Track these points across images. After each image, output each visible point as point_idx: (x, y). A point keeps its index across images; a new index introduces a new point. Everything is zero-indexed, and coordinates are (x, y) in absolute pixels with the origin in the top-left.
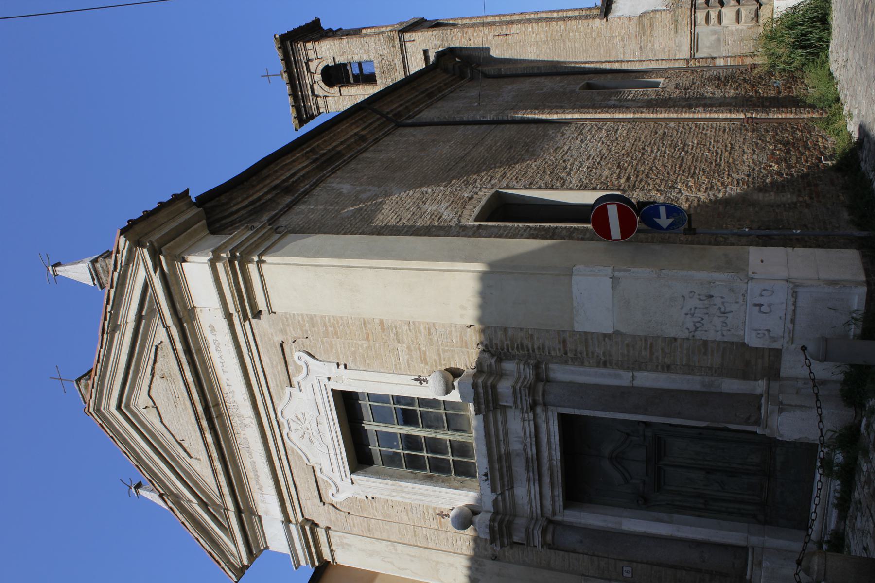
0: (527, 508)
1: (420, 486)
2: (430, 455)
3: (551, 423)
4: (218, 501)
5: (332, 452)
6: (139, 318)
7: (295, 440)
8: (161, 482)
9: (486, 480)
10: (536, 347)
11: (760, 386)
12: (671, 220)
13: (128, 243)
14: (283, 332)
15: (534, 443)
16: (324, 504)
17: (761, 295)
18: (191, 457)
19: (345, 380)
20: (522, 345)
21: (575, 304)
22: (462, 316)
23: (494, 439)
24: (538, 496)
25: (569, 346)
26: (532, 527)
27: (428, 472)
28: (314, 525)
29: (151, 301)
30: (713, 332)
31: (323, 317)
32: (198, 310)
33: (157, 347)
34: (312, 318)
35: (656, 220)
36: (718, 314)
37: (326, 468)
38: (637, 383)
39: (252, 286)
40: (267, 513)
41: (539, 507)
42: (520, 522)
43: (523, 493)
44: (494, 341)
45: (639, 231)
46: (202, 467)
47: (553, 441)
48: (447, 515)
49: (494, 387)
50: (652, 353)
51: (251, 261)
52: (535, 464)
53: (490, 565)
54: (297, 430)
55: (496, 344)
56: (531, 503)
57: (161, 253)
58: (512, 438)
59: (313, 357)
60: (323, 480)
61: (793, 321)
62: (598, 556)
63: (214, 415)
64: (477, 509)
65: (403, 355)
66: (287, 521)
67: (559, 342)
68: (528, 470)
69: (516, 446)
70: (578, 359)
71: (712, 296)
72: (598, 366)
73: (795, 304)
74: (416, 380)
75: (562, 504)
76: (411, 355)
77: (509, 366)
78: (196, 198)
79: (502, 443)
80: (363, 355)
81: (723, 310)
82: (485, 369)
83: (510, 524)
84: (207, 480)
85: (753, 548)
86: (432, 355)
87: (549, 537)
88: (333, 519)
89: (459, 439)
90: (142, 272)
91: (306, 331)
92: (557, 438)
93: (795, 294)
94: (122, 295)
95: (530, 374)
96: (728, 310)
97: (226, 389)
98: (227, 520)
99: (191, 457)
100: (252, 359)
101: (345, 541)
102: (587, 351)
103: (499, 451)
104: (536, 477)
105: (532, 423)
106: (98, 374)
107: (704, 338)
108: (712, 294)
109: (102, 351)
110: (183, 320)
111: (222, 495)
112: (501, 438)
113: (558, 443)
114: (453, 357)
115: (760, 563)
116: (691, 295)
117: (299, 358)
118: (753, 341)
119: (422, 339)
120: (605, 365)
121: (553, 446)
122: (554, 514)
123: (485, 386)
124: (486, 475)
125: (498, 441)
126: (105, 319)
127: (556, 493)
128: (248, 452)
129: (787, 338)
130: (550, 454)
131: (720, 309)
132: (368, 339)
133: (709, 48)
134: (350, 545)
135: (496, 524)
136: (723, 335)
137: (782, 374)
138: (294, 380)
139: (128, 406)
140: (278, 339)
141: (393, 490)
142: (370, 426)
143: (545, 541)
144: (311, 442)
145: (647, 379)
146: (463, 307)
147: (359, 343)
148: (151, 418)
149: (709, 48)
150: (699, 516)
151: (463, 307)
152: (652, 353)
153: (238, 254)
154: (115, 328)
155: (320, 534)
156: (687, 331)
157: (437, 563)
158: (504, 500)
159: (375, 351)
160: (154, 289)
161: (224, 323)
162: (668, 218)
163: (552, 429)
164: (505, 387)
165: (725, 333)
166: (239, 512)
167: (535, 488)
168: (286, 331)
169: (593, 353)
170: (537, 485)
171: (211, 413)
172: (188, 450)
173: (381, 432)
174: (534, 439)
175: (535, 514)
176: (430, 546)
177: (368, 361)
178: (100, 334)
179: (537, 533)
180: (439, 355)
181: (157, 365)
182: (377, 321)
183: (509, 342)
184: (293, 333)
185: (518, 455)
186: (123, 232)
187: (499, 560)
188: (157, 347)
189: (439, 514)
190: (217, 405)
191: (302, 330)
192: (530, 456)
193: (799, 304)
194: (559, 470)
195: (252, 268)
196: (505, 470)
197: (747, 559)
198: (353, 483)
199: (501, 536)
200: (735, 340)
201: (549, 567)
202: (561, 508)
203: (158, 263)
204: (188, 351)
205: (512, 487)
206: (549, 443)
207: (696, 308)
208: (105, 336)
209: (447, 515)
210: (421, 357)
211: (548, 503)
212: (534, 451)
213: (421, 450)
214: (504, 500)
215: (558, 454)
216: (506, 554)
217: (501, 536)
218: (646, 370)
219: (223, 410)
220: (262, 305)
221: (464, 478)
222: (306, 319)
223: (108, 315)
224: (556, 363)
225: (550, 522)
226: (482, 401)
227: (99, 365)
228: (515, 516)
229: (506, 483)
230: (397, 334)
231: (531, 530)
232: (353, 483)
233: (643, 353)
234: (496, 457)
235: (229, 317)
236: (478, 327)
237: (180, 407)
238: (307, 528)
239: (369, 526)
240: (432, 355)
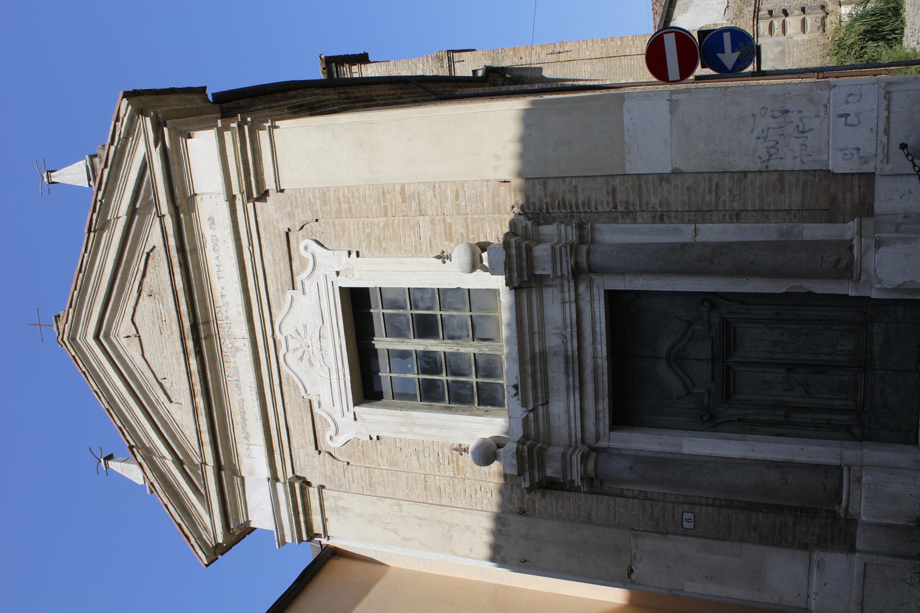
0: (564, 431)
1: (435, 414)
2: (450, 378)
3: (596, 303)
4: (197, 461)
5: (334, 376)
6: (133, 211)
7: (293, 365)
8: (132, 431)
9: (516, 394)
10: (580, 202)
11: (849, 229)
12: (737, 54)
13: (130, 107)
14: (291, 215)
15: (575, 334)
16: (320, 452)
17: (847, 102)
18: (171, 402)
19: (356, 274)
20: (564, 202)
21: (626, 138)
22: (495, 168)
23: (526, 330)
24: (578, 411)
25: (620, 197)
26: (569, 453)
27: (446, 404)
28: (306, 483)
29: (147, 190)
30: (790, 159)
31: (337, 190)
32: (198, 198)
33: (148, 255)
34: (324, 193)
35: (719, 55)
36: (796, 134)
37: (326, 400)
38: (700, 238)
39: (260, 159)
40: (251, 473)
41: (579, 429)
42: (555, 451)
43: (561, 409)
44: (532, 200)
45: (699, 78)
46: (183, 415)
47: (598, 330)
48: (466, 450)
49: (529, 250)
50: (717, 198)
51: (264, 129)
52: (575, 362)
53: (517, 523)
54: (295, 350)
55: (534, 204)
56: (569, 422)
57: (166, 126)
58: (549, 330)
59: (322, 246)
60: (321, 417)
61: (887, 132)
62: (652, 500)
63: (202, 335)
64: (501, 442)
65: (425, 231)
66: (274, 479)
67: (608, 193)
68: (567, 373)
69: (553, 342)
70: (629, 214)
71: (787, 111)
72: (654, 222)
73: (888, 108)
74: (439, 257)
75: (607, 422)
76: (434, 230)
77: (548, 230)
78: (214, 95)
79: (536, 337)
80: (379, 237)
81: (801, 129)
82: (520, 231)
83: (542, 452)
84: (187, 432)
85: (849, 468)
86: (458, 228)
87: (591, 465)
88: (329, 473)
89: (486, 350)
90: (143, 148)
91: (317, 211)
92: (603, 326)
93: (888, 95)
94: (116, 179)
95: (572, 235)
96: (807, 127)
97: (219, 301)
98: (204, 478)
99: (171, 402)
100: (251, 244)
101: (341, 503)
102: (640, 201)
104: (577, 384)
105: (573, 305)
106: (78, 288)
107: (780, 168)
108: (787, 108)
109: (86, 255)
110: (181, 209)
111: (201, 444)
112: (536, 329)
113: (604, 332)
114: (483, 228)
115: (859, 480)
116: (763, 112)
117: (306, 248)
118: (839, 165)
119: (449, 207)
120: (662, 220)
121: (598, 338)
122: (598, 438)
123: (518, 247)
124: (516, 387)
125: (532, 334)
126: (94, 211)
127: (601, 407)
128: (237, 386)
129: (881, 156)
130: (595, 349)
131: (798, 127)
132: (386, 215)
133: (773, 60)
134: (345, 509)
135: (526, 448)
136: (803, 162)
137: (875, 211)
138: (298, 279)
139: (107, 336)
140: (283, 227)
141: (403, 424)
142: (382, 343)
143: (585, 469)
144: (311, 364)
145: (713, 232)
146: (497, 157)
147: (376, 220)
148: (131, 351)
149: (773, 60)
150: (778, 435)
151: (497, 157)
152: (717, 198)
153: (249, 119)
154: (104, 225)
155: (311, 496)
156: (759, 161)
157: (451, 526)
158: (536, 419)
159: (393, 230)
160: (152, 172)
161: (225, 206)
162: (733, 51)
163: (597, 313)
164: (541, 252)
165: (805, 159)
166: (219, 468)
167: (575, 400)
168: (293, 214)
169: (647, 204)
170: (577, 396)
171: (199, 334)
172: (169, 393)
173: (394, 350)
174: (575, 329)
175: (574, 440)
176: (443, 503)
177: (384, 245)
178: (86, 231)
179: (576, 458)
180: (467, 226)
181: (146, 280)
182: (398, 188)
183: (549, 200)
184: (301, 215)
185: (555, 354)
186: (127, 95)
187: (527, 515)
188: (148, 255)
189: (456, 450)
190: (207, 323)
191: (311, 210)
192: (570, 353)
193: (894, 108)
194: (605, 371)
195: (263, 136)
196: (539, 376)
197: (841, 479)
198: (355, 419)
199: (533, 357)
200: (817, 167)
201: (589, 521)
202: (607, 429)
203: (160, 136)
204: (181, 249)
205: (547, 403)
206: (594, 332)
207: (768, 129)
208: (92, 234)
209: (466, 450)
210: (445, 232)
213: (439, 372)
214: (536, 419)
215: (605, 348)
216: (537, 506)
217: (532, 466)
218: (711, 222)
219: (214, 330)
220: (270, 184)
221: (489, 407)
222: (318, 195)
223: (98, 204)
224: (604, 222)
225: (593, 449)
226: (515, 266)
227: (81, 275)
228: (550, 445)
229: (540, 395)
230: (419, 204)
231: (568, 456)
232: (355, 419)
233: (707, 198)
234: (528, 356)
235: (231, 199)
236: (516, 182)
237: (166, 333)
238: (297, 485)
239: (371, 478)
240: (458, 228)
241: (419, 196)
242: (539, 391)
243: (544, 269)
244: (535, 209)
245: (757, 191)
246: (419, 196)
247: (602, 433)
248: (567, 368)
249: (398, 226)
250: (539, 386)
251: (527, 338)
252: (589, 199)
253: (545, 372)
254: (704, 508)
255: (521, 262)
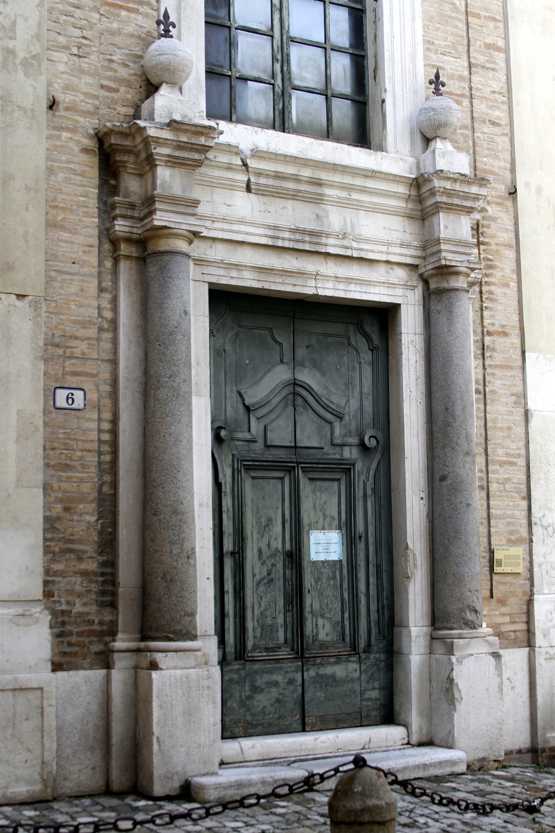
10: (493, 288)
15: (349, 253)
47: (352, 287)
50: (502, 464)
55: (488, 227)
67: (503, 326)
79: (344, 194)
103: (331, 185)
104: (280, 243)
105: (384, 257)
121: (341, 286)
122: (200, 262)
130: (327, 278)
152: (502, 464)
156: (541, 515)
163: (372, 289)
170: (263, 241)
183: (494, 247)
185: (318, 216)
194: (298, 290)
196: (291, 185)
202: (214, 280)
211: (218, 253)
212: (332, 250)
214: (229, 168)
217: (180, 146)
241: (493, 69)
242: (270, 182)
243: (446, 227)
244: (483, 227)
245: (509, 512)
246: (493, 69)
247: (206, 270)
248: (303, 232)
249: (456, 27)
250: (278, 183)
251: (347, 180)
252: (496, 300)
253: (294, 196)
254: (94, 425)
255: (459, 197)
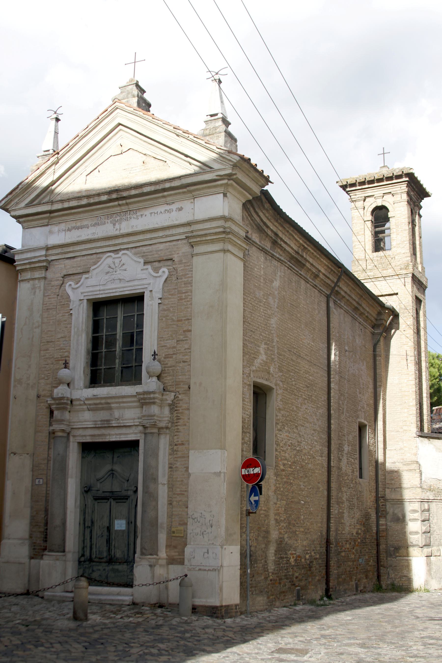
2: (104, 353)
5: (102, 288)
10: (179, 427)
14: (180, 262)
15: (120, 425)
18: (87, 176)
21: (205, 451)
25: (180, 448)
26: (65, 423)
28: (47, 269)
30: (192, 528)
34: (190, 283)
37: (90, 282)
38: (160, 486)
42: (67, 415)
44: (181, 402)
47: (122, 436)
49: (154, 403)
52: (106, 425)
55: (179, 403)
56: (80, 422)
60: (81, 278)
61: (200, 570)
62: (48, 463)
66: (48, 249)
67: (182, 441)
68: (102, 421)
70: (173, 452)
71: (212, 527)
72: (169, 464)
74: (155, 352)
76: (169, 348)
77: (167, 411)
79: (118, 405)
81: (204, 533)
83: (65, 409)
87: (60, 434)
88: (53, 283)
91: (182, 279)
93: (214, 570)
95: (163, 424)
101: (37, 291)
102: (178, 457)
103: (113, 403)
104: (97, 426)
105: (132, 424)
108: (213, 527)
112: (122, 405)
114: (170, 376)
115: (57, 560)
118: (188, 550)
119: (180, 357)
120: (170, 468)
121: (118, 437)
122: (74, 436)
125: (119, 403)
129: (190, 567)
130: (113, 435)
131: (205, 531)
133: (393, 513)
135: (65, 401)
136: (190, 534)
138: (149, 267)
140: (176, 258)
147: (176, 314)
149: (393, 513)
150: (80, 524)
156: (192, 514)
158: (81, 405)
159: (171, 325)
161: (184, 220)
163: (129, 436)
165: (192, 534)
168: (181, 264)
169: (177, 461)
170: (92, 426)
173: (117, 321)
174: (122, 425)
175: (72, 424)
177: (164, 319)
179: (63, 427)
180: (171, 367)
183: (181, 411)
185: (111, 414)
187: (37, 399)
189: (66, 361)
191: (182, 275)
193: (209, 572)
196: (100, 406)
202: (78, 441)
205: (89, 410)
206: (120, 434)
207: (205, 518)
211: (81, 432)
212: (114, 425)
213: (106, 348)
214: (81, 405)
215: (114, 440)
217: (58, 404)
218: (168, 491)
220: (197, 249)
224: (170, 439)
225: (69, 434)
226: (145, 396)
229: (92, 407)
233: (178, 490)
235: (189, 224)
241: (186, 340)
242: (94, 406)
243: (145, 411)
244: (177, 404)
245: (180, 513)
246: (186, 340)
247: (76, 438)
248: (104, 421)
249: (173, 328)
250: (96, 406)
251: (117, 400)
252: (180, 432)
253: (103, 409)
254: (45, 489)
255: (148, 399)
